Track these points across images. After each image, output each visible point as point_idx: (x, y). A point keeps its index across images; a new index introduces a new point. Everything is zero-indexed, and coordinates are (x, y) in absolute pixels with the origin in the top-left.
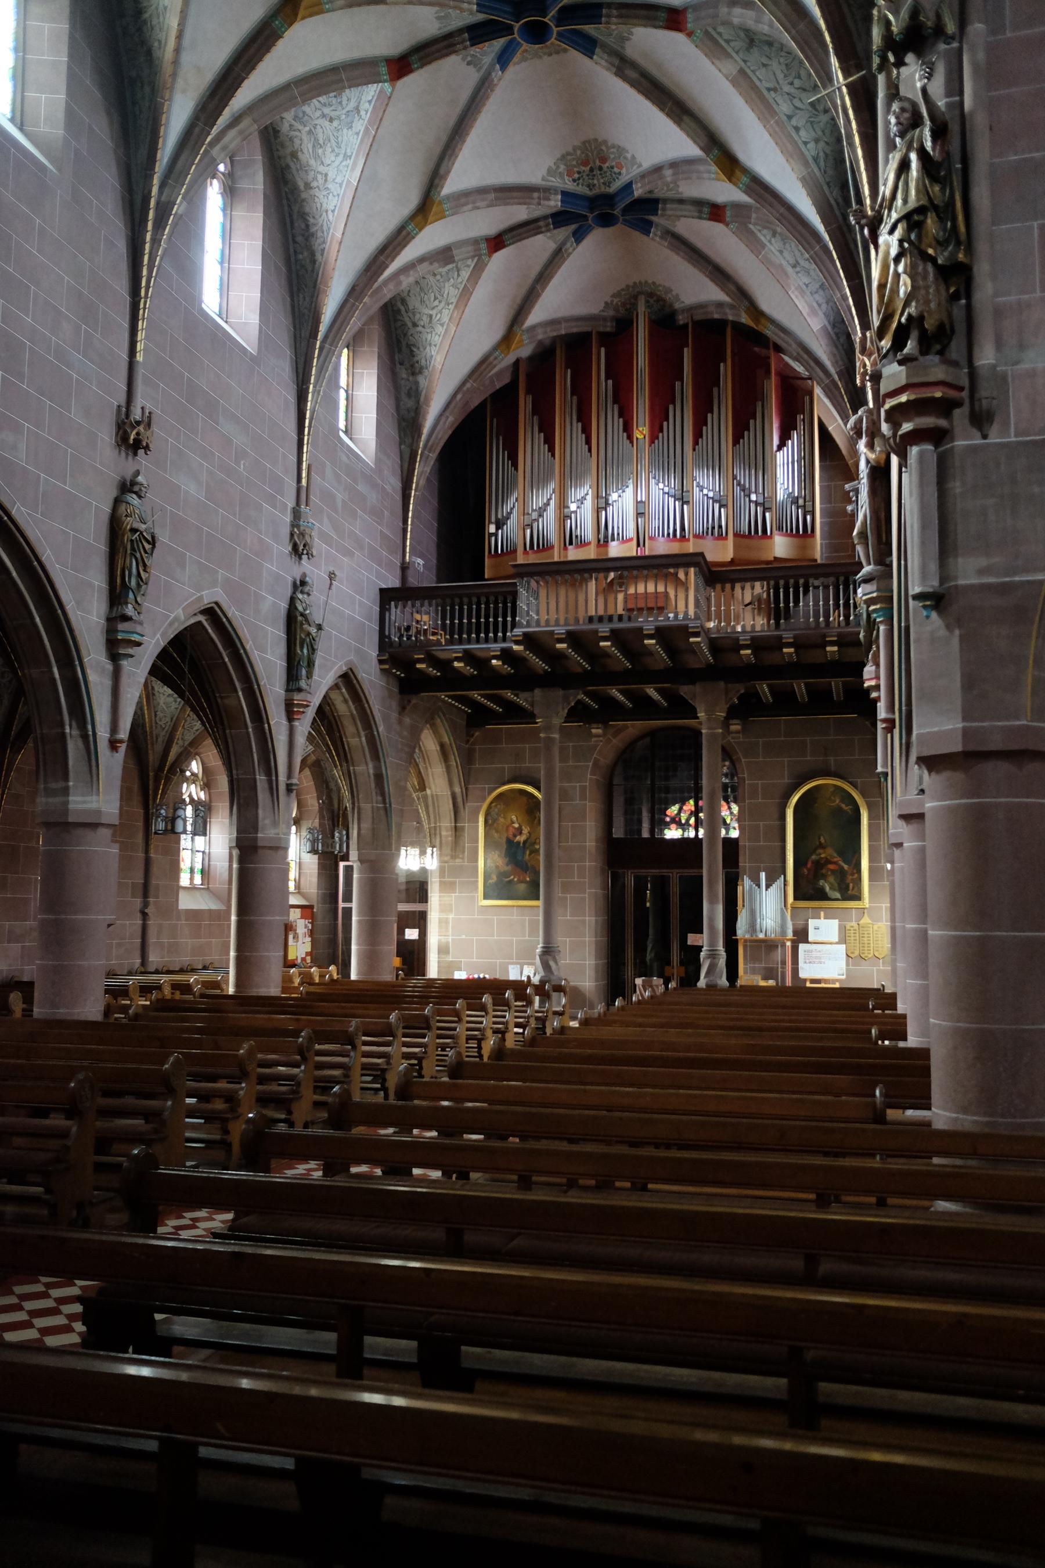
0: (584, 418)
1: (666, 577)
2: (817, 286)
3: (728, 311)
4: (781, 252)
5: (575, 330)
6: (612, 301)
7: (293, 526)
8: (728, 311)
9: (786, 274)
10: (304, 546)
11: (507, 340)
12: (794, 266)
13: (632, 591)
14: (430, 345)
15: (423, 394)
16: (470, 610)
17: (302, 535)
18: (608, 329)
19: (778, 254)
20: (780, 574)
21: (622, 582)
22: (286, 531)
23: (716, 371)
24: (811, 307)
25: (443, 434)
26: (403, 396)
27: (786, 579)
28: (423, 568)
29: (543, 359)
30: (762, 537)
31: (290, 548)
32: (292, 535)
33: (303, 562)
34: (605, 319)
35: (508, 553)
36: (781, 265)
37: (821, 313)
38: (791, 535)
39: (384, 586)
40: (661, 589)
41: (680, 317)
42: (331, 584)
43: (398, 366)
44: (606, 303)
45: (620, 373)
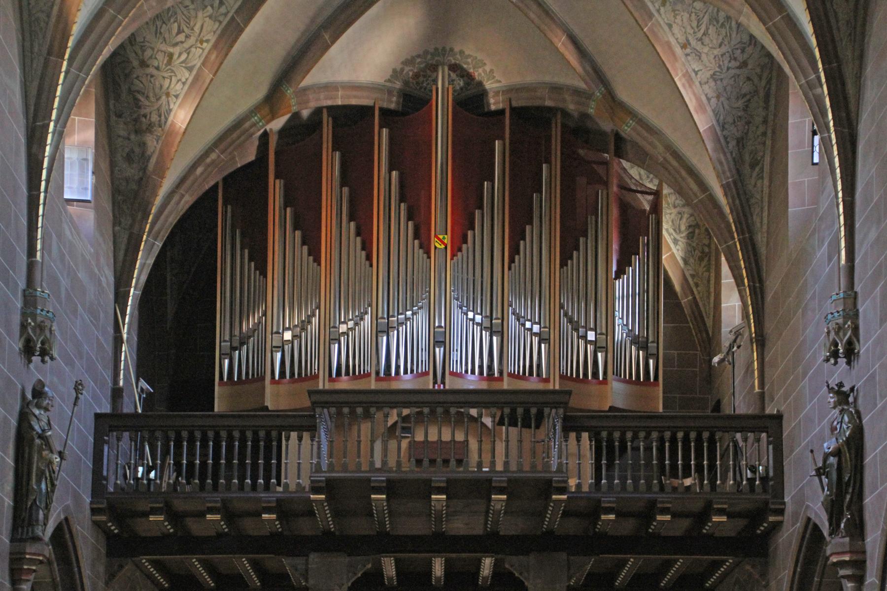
0: (359, 212)
1: (461, 420)
2: (708, 74)
3: (568, 97)
4: (670, 26)
5: (354, 102)
6: (402, 70)
7: (24, 315)
8: (568, 97)
9: (673, 54)
10: (43, 343)
11: (272, 101)
12: (684, 47)
13: (419, 437)
14: (168, 95)
15: (153, 160)
16: (243, 446)
17: (41, 327)
18: (392, 106)
19: (666, 28)
20: (654, 424)
21: (405, 426)
22: (17, 319)
23: (540, 166)
24: (698, 100)
25: (172, 218)
26: (119, 158)
27: (611, 436)
28: (137, 393)
29: (302, 131)
30: (582, 381)
31: (21, 345)
32: (24, 326)
33: (32, 366)
34: (390, 92)
35: (254, 380)
36: (668, 44)
37: (709, 109)
38: (629, 382)
39: (99, 411)
40: (460, 437)
41: (492, 101)
42: (77, 398)
43: (113, 118)
44: (394, 71)
45: (410, 162)
